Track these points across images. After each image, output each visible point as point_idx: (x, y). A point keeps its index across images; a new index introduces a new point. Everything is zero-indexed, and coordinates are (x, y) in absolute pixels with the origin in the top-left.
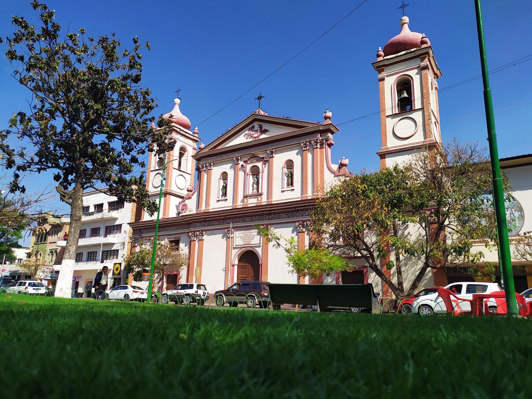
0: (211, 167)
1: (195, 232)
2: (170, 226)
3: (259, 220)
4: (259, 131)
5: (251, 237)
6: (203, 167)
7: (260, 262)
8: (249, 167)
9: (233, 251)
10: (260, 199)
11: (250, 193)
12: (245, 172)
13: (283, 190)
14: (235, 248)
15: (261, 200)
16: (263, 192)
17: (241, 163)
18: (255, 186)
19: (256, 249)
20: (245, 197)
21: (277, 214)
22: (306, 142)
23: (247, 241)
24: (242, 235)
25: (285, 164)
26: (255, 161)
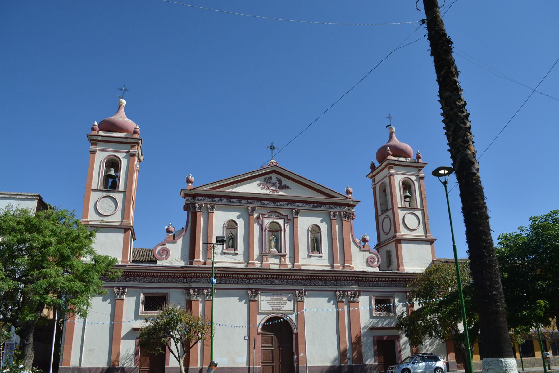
0: (213, 210)
2: (148, 276)
4: (278, 185)
5: (282, 302)
6: (201, 207)
7: (295, 331)
8: (267, 222)
9: (258, 316)
10: (283, 260)
13: (310, 255)
16: (286, 253)
18: (273, 244)
20: (264, 255)
21: (313, 280)
22: (336, 212)
23: (277, 307)
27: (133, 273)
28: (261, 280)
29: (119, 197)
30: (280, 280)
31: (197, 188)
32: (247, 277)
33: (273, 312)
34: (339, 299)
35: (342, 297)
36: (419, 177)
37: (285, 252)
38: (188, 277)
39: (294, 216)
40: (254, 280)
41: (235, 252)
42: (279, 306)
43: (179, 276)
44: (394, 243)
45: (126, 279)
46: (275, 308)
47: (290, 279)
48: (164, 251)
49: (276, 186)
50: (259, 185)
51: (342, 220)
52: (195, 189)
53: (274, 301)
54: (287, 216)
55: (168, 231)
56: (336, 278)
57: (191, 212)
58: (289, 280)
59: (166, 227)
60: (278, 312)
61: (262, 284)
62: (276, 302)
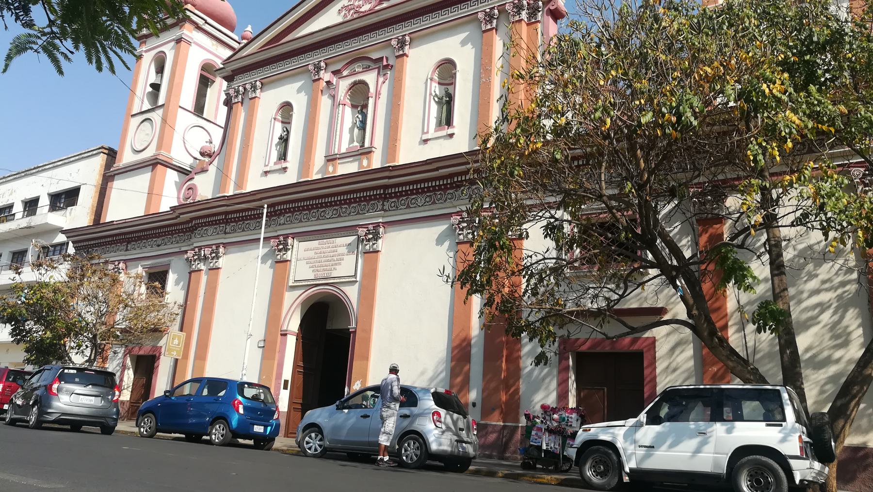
1: (200, 248)
2: (150, 238)
3: (358, 213)
5: (335, 258)
8: (343, 85)
11: (343, 150)
12: (333, 97)
13: (425, 137)
14: (293, 288)
15: (369, 164)
16: (375, 144)
17: (326, 76)
18: (356, 131)
19: (344, 288)
20: (328, 161)
23: (324, 270)
24: (311, 254)
25: (434, 71)
26: (361, 70)
29: (157, 116)
30: (334, 208)
33: (315, 283)
39: (397, 54)
42: (328, 267)
45: (127, 247)
56: (456, 180)
58: (352, 206)
61: (301, 221)
62: (323, 259)
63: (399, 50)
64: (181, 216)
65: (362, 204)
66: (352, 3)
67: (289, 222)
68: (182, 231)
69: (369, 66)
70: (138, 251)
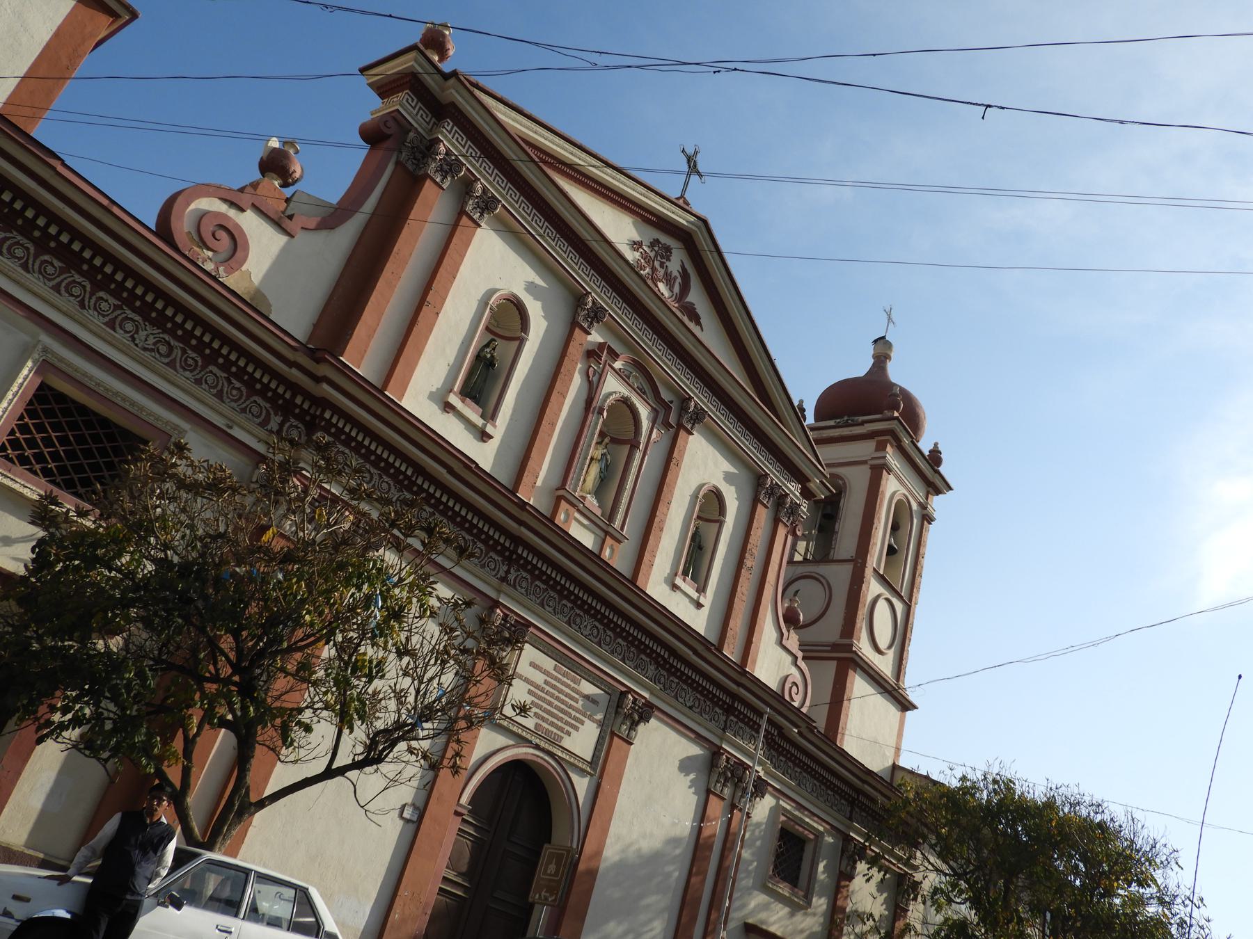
0: (482, 214)
2: (116, 294)
4: (677, 289)
5: (573, 713)
13: (679, 581)
16: (624, 533)
19: (575, 778)
23: (552, 724)
24: (539, 678)
27: (48, 225)
28: (545, 590)
30: (597, 624)
31: (477, 86)
32: (508, 549)
34: (718, 781)
35: (726, 780)
36: (925, 512)
37: (622, 529)
38: (296, 417)
40: (525, 574)
41: (486, 425)
42: (560, 724)
43: (258, 386)
44: (835, 663)
46: (544, 725)
47: (625, 639)
48: (222, 234)
49: (671, 289)
50: (636, 245)
51: (776, 521)
52: (468, 85)
53: (552, 696)
54: (667, 407)
55: (275, 165)
57: (398, 163)
58: (620, 640)
59: (275, 143)
60: (547, 747)
62: (556, 703)
63: (689, 421)
64: (325, 386)
65: (632, 649)
66: (652, 254)
67: (523, 591)
68: (250, 383)
69: (644, 393)
70: (33, 280)
